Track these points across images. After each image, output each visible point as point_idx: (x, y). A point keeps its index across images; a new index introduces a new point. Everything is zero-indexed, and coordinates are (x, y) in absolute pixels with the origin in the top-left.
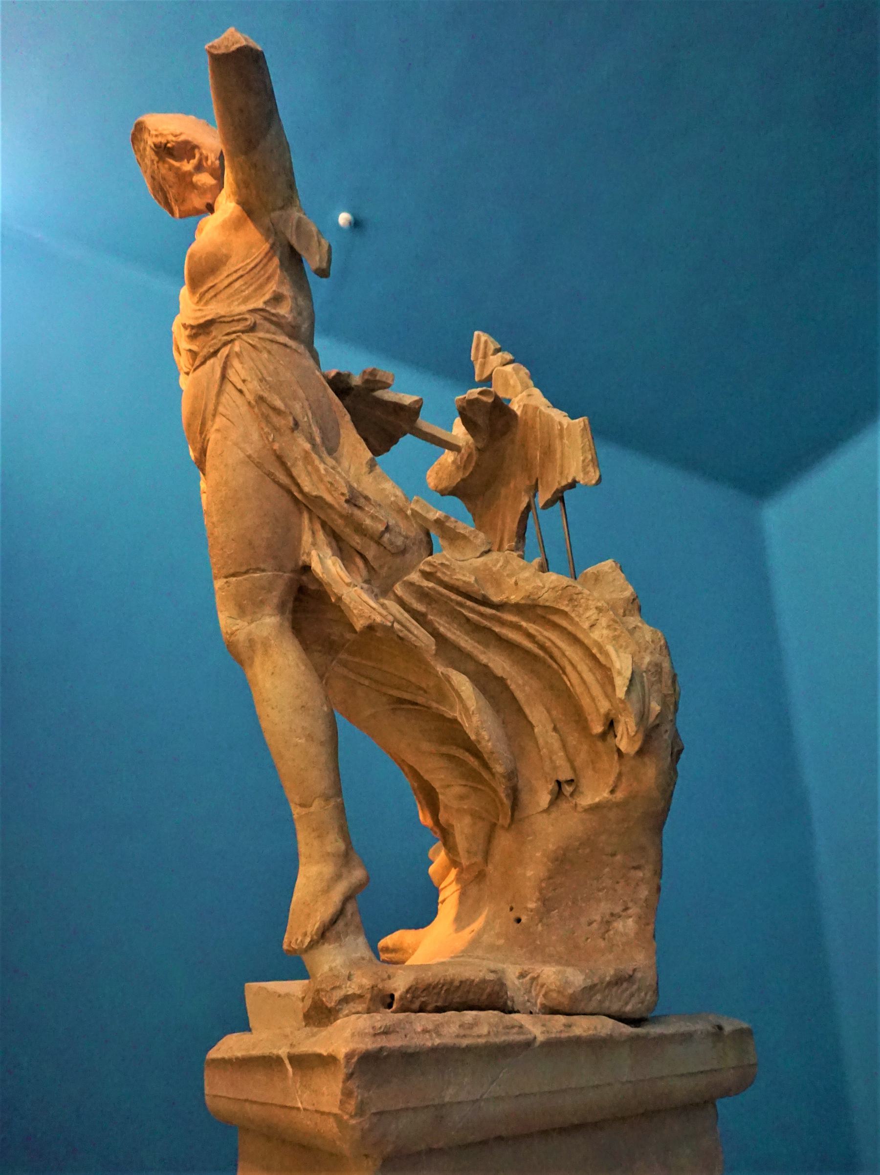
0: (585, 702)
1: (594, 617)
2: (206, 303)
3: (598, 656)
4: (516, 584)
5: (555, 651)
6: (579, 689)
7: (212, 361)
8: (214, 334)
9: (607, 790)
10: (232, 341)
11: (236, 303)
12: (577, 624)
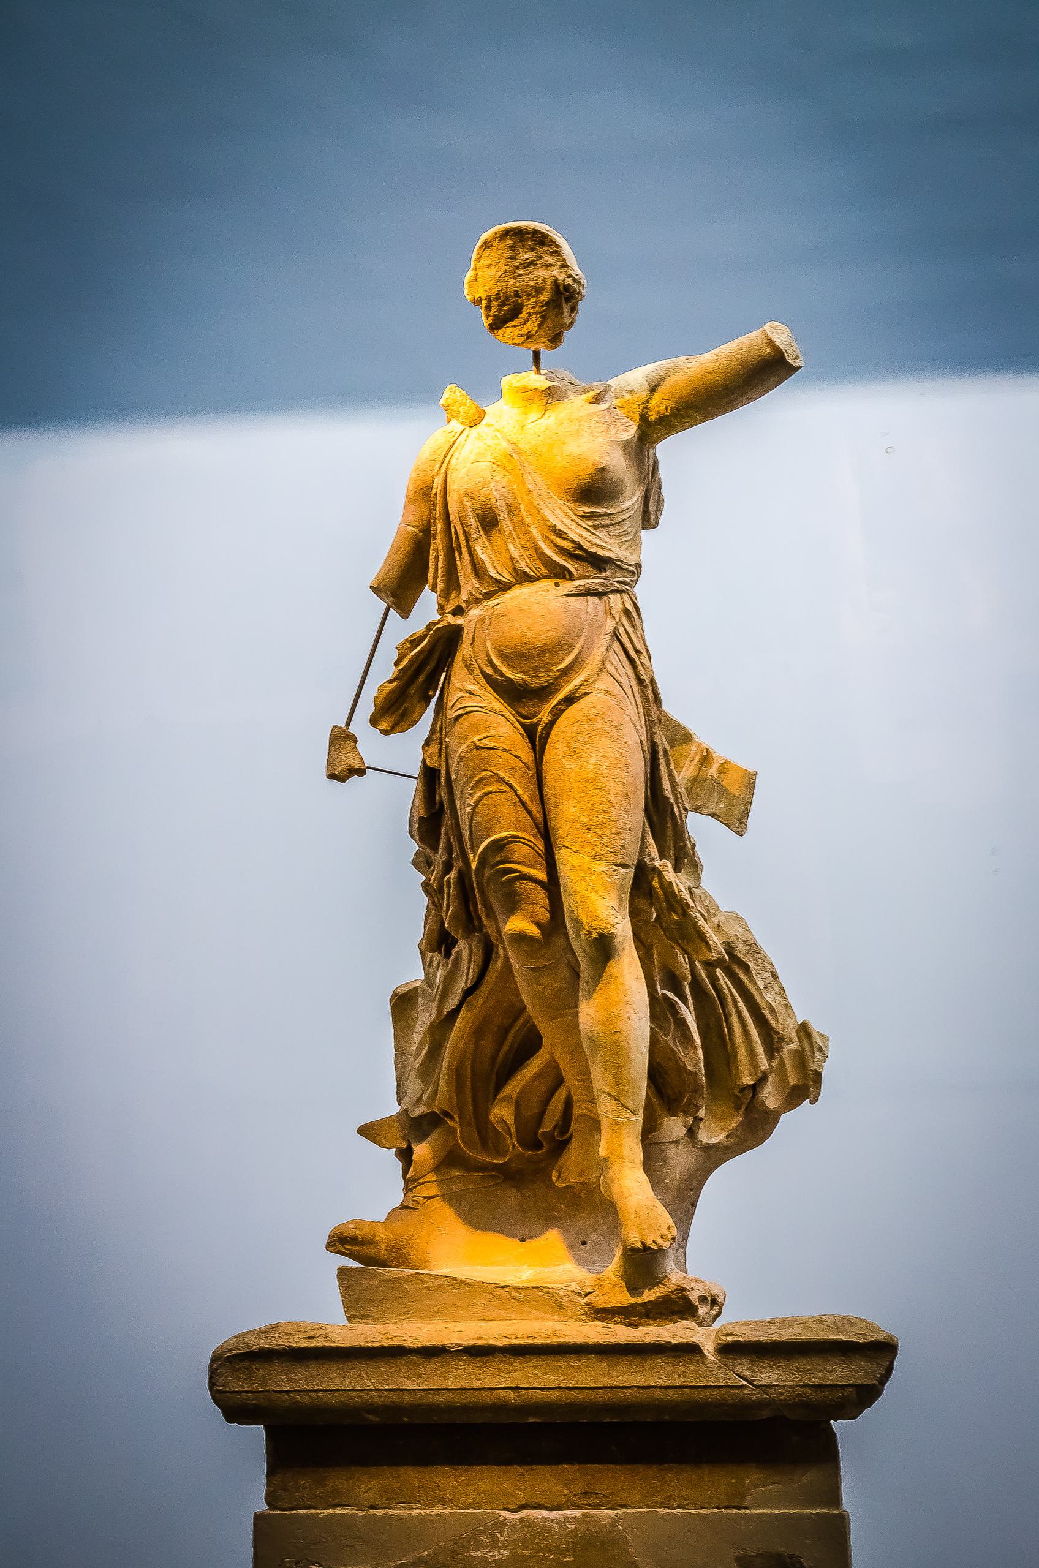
0: (742, 1053)
1: (768, 981)
2: (594, 526)
3: (769, 1017)
4: (719, 926)
5: (729, 998)
6: (739, 1039)
7: (596, 599)
8: (608, 574)
9: (725, 1134)
10: (621, 592)
11: (625, 546)
12: (754, 982)
